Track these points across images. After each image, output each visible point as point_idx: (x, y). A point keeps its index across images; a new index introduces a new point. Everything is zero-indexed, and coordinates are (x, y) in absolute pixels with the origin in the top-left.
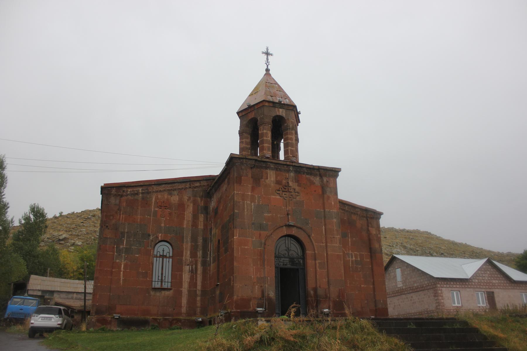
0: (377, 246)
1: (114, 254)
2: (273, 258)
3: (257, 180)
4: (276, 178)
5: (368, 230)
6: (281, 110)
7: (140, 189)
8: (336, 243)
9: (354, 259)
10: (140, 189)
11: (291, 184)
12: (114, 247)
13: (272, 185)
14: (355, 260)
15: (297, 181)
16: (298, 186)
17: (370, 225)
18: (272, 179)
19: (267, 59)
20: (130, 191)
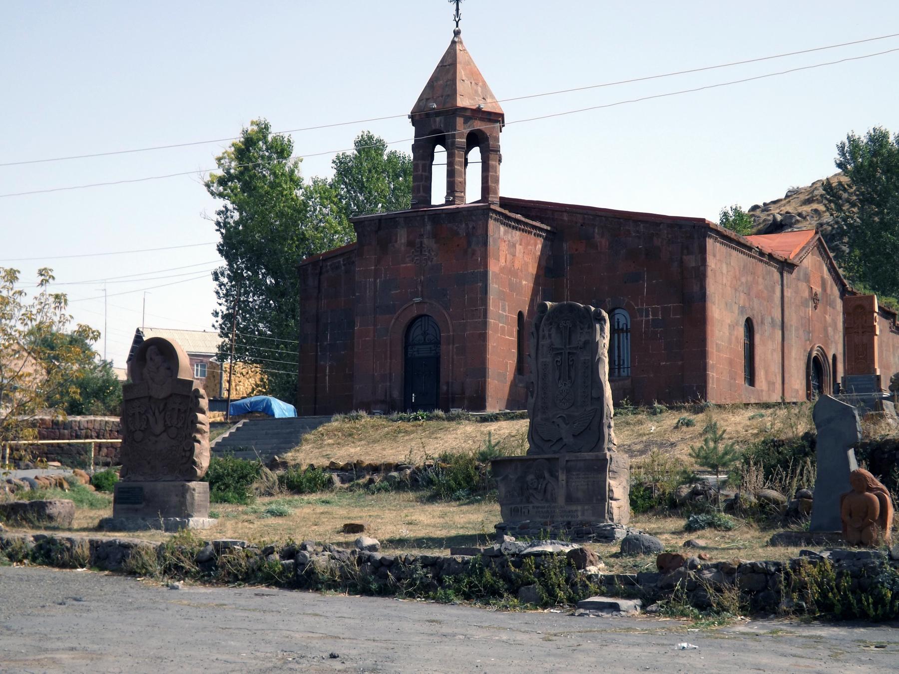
0: (696, 288)
1: (317, 355)
2: (399, 348)
3: (385, 244)
4: (408, 237)
5: (681, 262)
6: (438, 119)
7: (341, 260)
8: (480, 317)
9: (651, 317)
10: (341, 260)
11: (425, 241)
12: (317, 346)
13: (403, 248)
14: (652, 319)
15: (435, 236)
16: (436, 243)
17: (685, 251)
18: (403, 241)
19: (457, 9)
20: (331, 265)
